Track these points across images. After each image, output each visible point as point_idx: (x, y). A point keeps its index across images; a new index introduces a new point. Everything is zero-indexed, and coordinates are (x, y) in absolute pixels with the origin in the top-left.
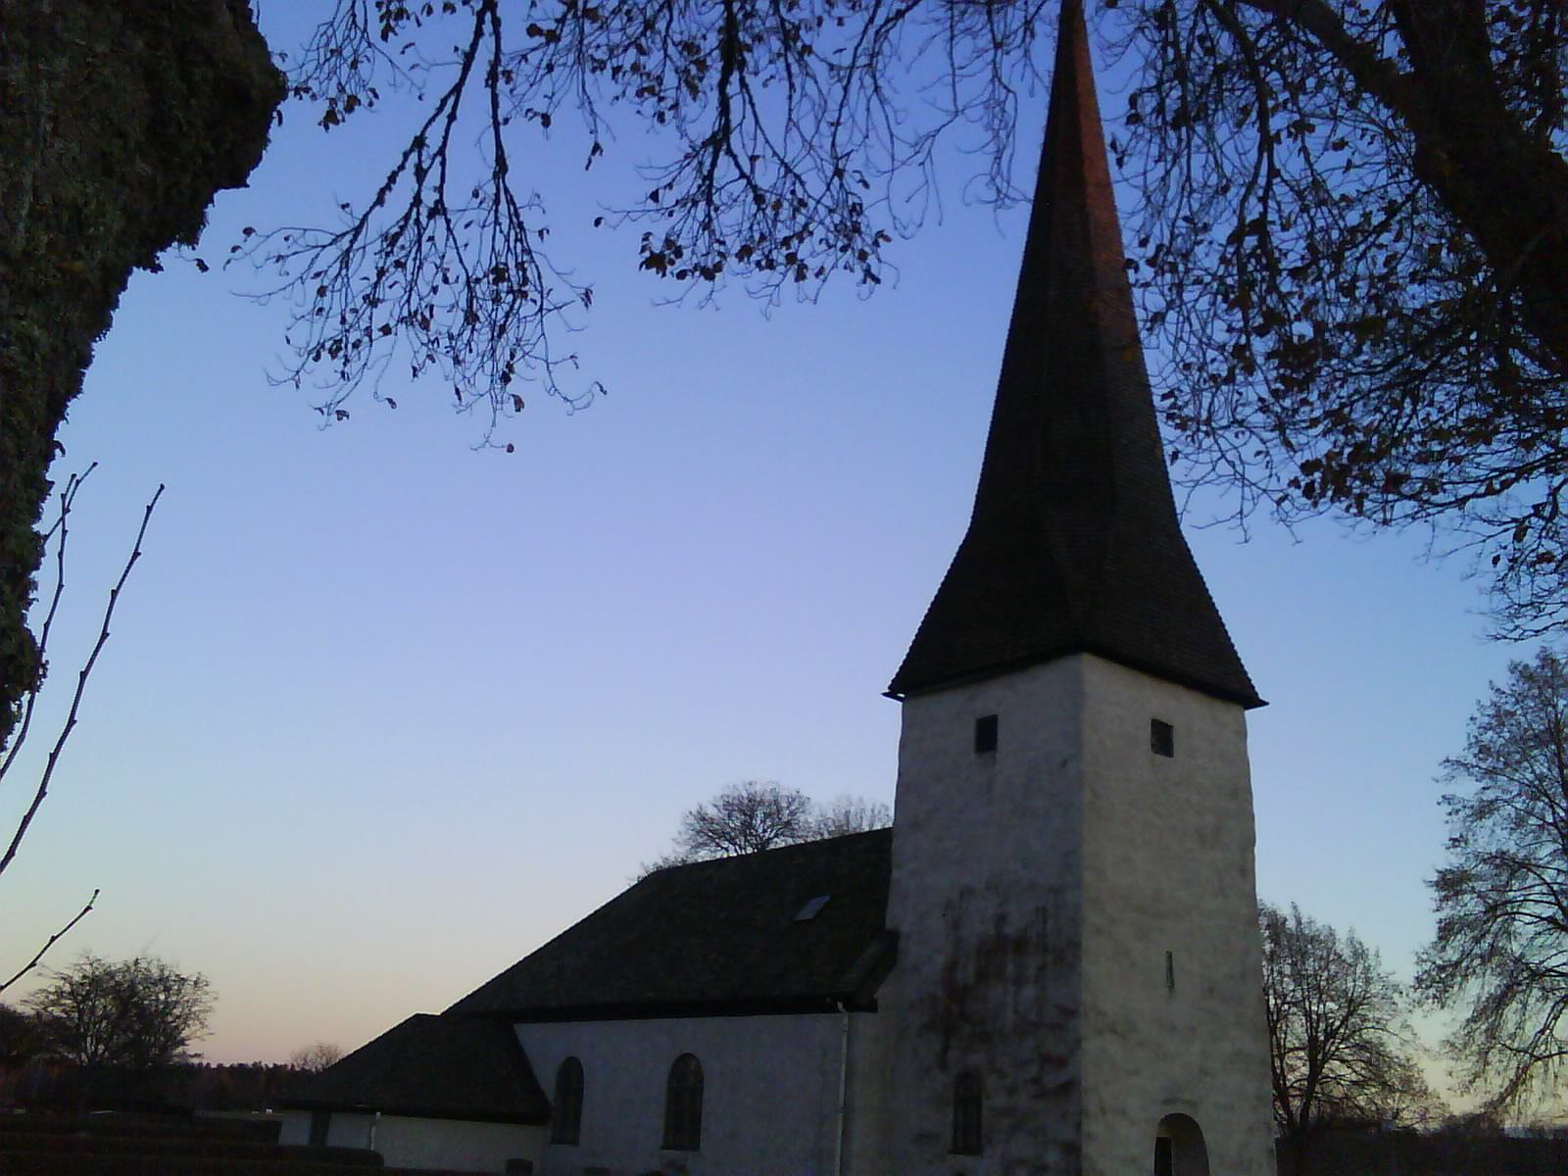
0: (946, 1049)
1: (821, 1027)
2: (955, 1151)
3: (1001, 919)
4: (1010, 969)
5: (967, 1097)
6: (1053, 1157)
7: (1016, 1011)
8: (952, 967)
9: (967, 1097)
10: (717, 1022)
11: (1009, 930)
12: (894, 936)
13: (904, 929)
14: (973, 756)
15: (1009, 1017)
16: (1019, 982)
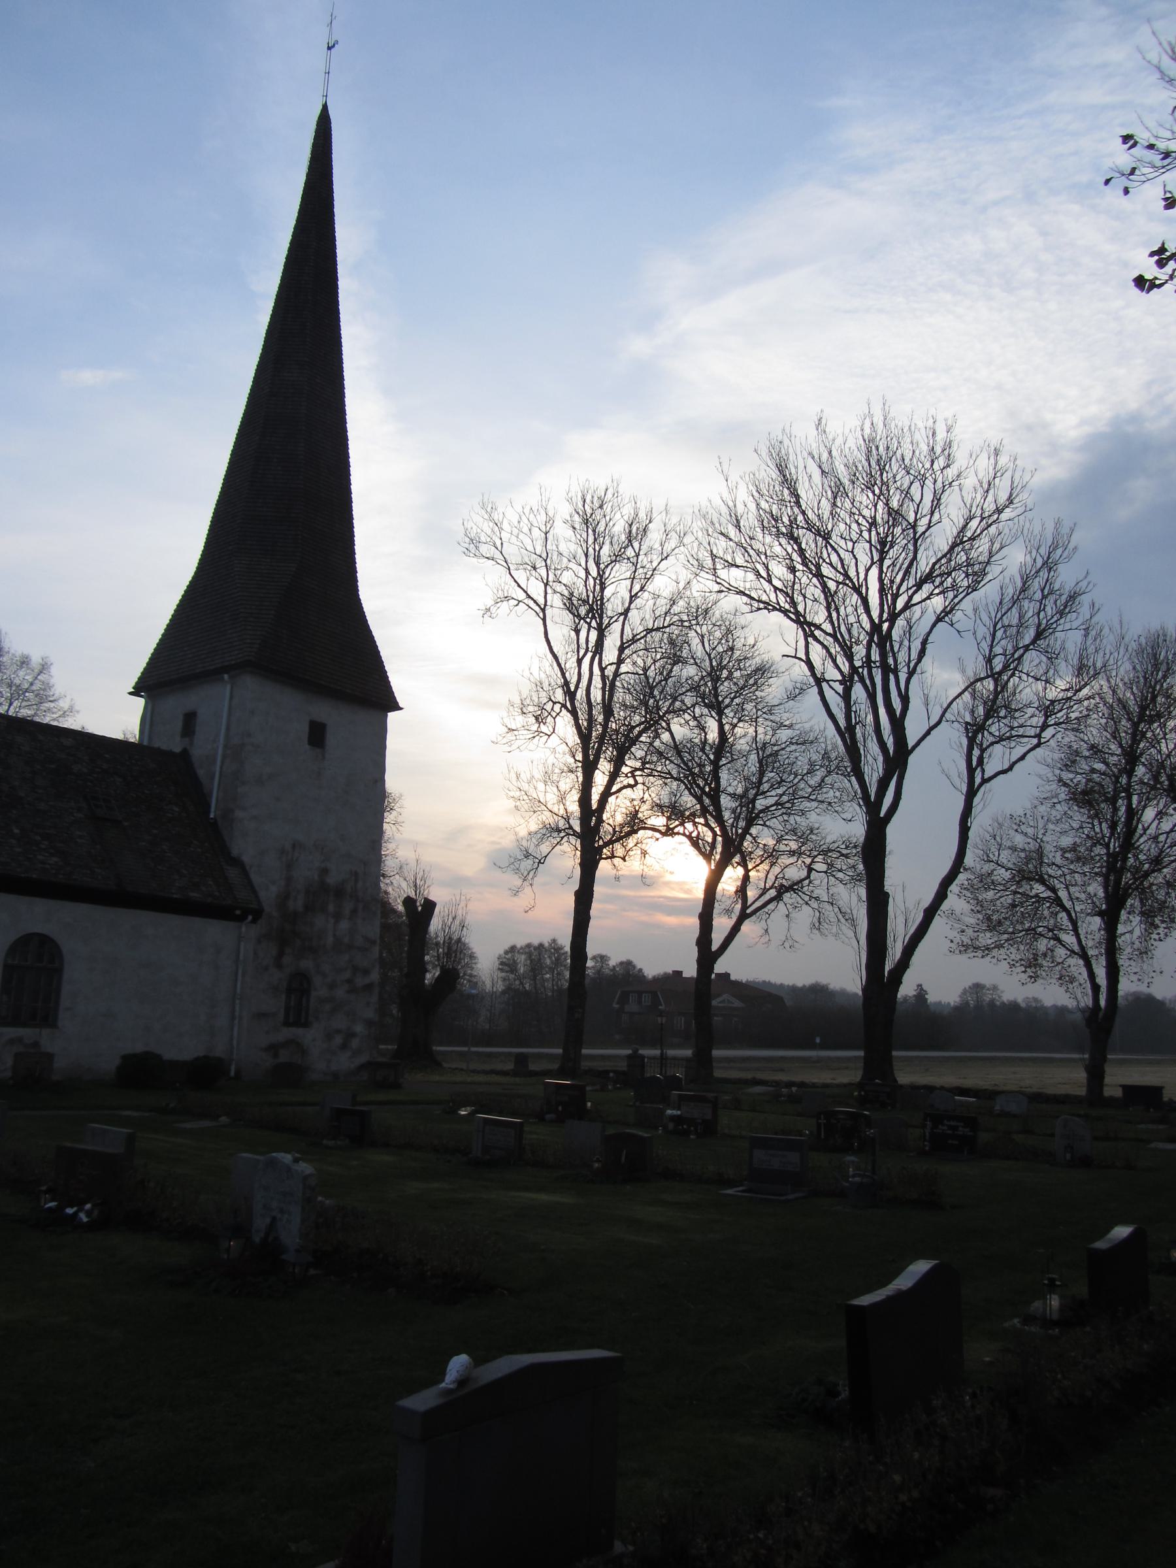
0: (281, 954)
1: (215, 931)
2: (287, 1023)
3: (325, 871)
4: (331, 908)
5: (298, 988)
6: (359, 1028)
7: (334, 935)
8: (284, 897)
9: (298, 988)
10: (81, 910)
11: (331, 880)
12: (237, 863)
13: (246, 859)
14: (307, 747)
15: (330, 940)
16: (338, 916)
